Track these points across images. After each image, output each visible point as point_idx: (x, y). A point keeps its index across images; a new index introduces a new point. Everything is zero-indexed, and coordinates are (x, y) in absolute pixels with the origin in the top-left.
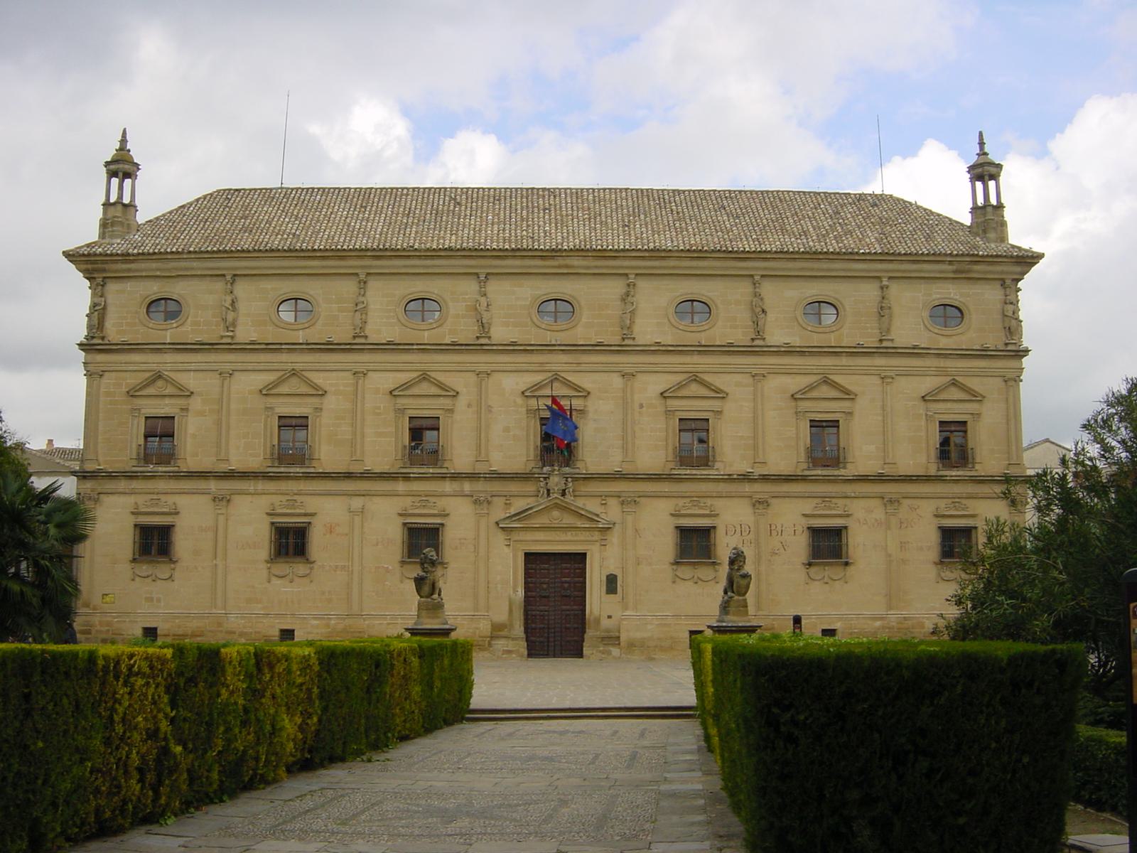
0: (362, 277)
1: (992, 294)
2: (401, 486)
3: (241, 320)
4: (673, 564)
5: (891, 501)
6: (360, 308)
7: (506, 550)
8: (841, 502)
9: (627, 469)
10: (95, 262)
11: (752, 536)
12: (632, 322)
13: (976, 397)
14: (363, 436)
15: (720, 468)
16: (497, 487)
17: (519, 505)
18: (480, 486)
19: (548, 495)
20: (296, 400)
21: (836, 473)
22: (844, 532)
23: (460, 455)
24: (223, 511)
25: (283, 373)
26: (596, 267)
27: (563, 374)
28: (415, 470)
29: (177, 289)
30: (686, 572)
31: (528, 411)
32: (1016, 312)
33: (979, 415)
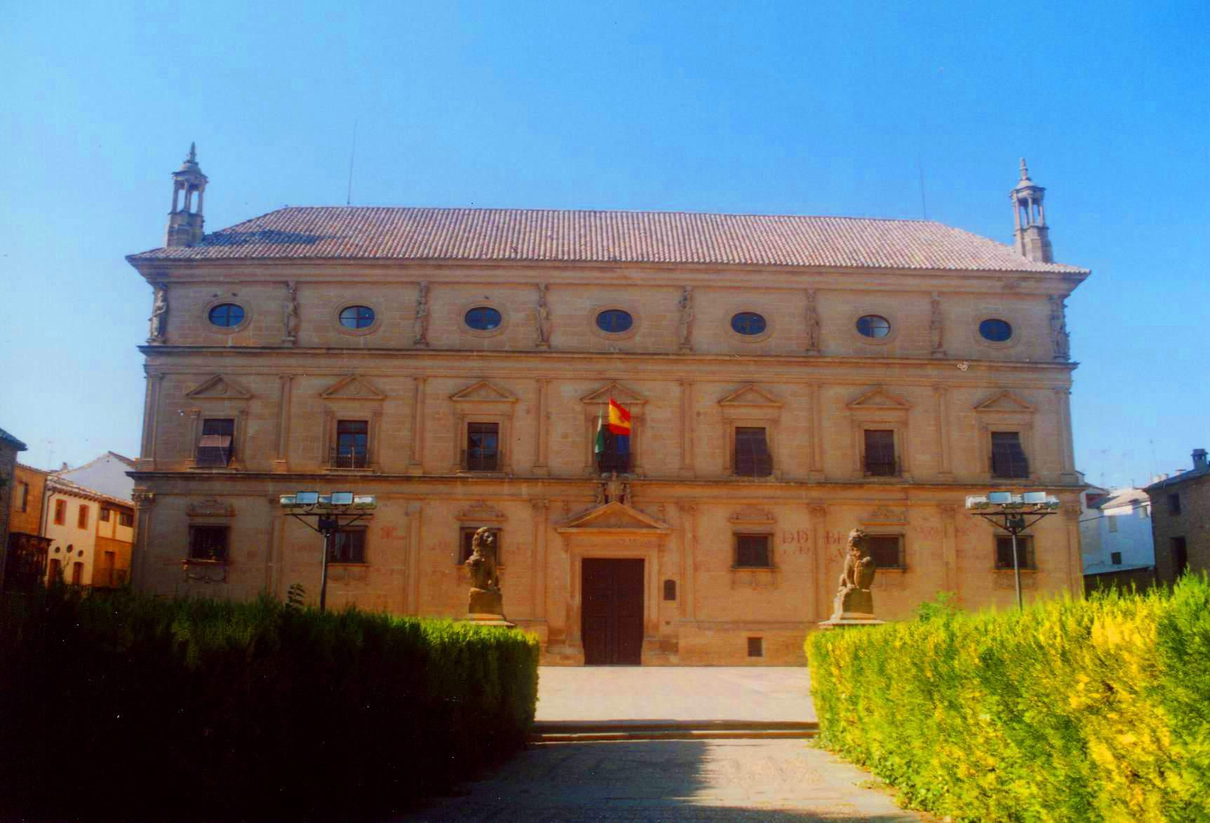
2: (459, 489)
3: (304, 325)
6: (424, 317)
7: (564, 555)
9: (685, 474)
10: (159, 267)
11: (810, 544)
12: (690, 333)
16: (556, 490)
17: (577, 508)
18: (538, 489)
22: (901, 542)
30: (744, 574)
32: (1063, 327)
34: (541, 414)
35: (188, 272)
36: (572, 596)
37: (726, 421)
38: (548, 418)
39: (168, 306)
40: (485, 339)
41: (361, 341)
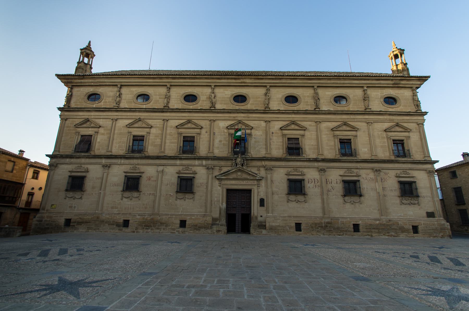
0: (169, 86)
1: (407, 93)
2: (178, 162)
3: (123, 101)
4: (287, 194)
5: (376, 171)
6: (168, 97)
7: (219, 188)
8: (355, 171)
9: (267, 156)
11: (319, 184)
12: (269, 103)
13: (407, 130)
14: (165, 143)
15: (305, 156)
16: (216, 162)
17: (225, 169)
18: (209, 162)
19: (236, 166)
20: (140, 129)
21: (353, 158)
22: (358, 183)
23: (202, 149)
24: (107, 171)
25: (134, 120)
26: (255, 83)
27: (243, 121)
28: (184, 156)
29: (100, 90)
30: (292, 197)
31: (229, 134)
33: (409, 137)
34: (212, 134)
35: (79, 81)
36: (222, 204)
37: (284, 135)
38: (214, 134)
39: (72, 94)
40: (191, 106)
41: (144, 107)
